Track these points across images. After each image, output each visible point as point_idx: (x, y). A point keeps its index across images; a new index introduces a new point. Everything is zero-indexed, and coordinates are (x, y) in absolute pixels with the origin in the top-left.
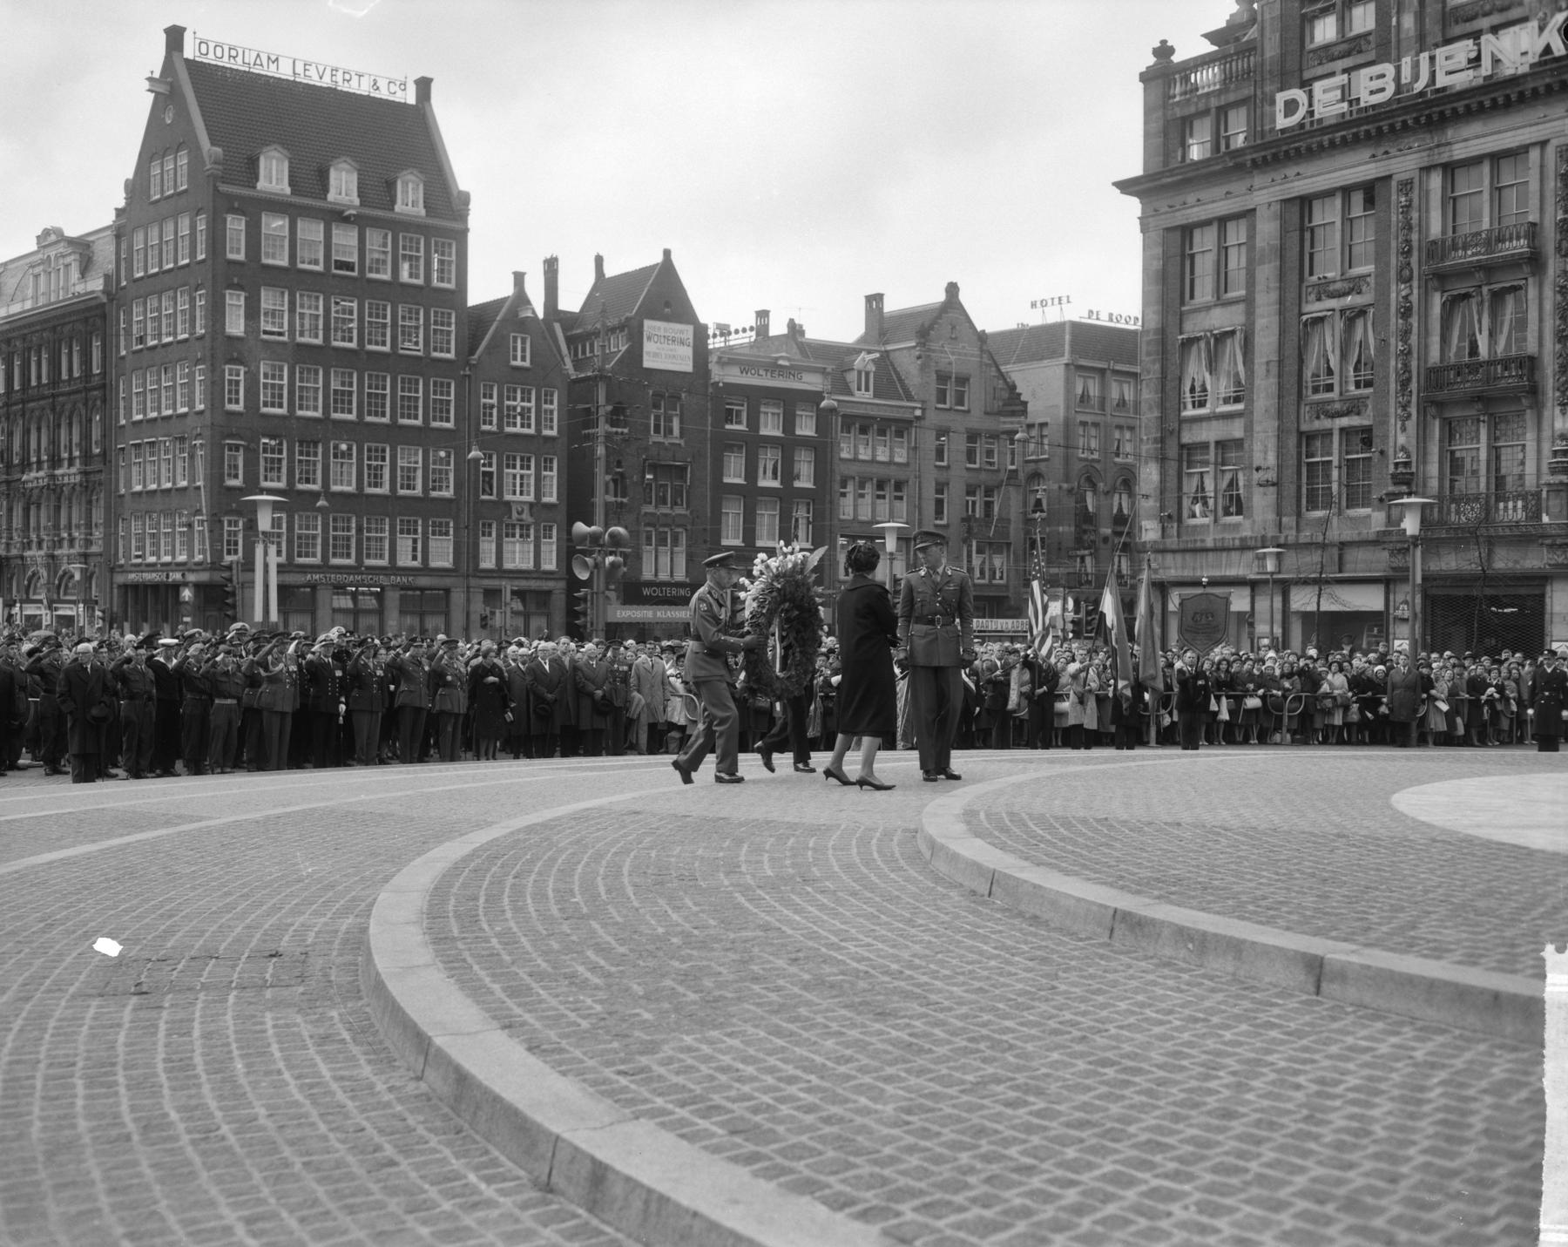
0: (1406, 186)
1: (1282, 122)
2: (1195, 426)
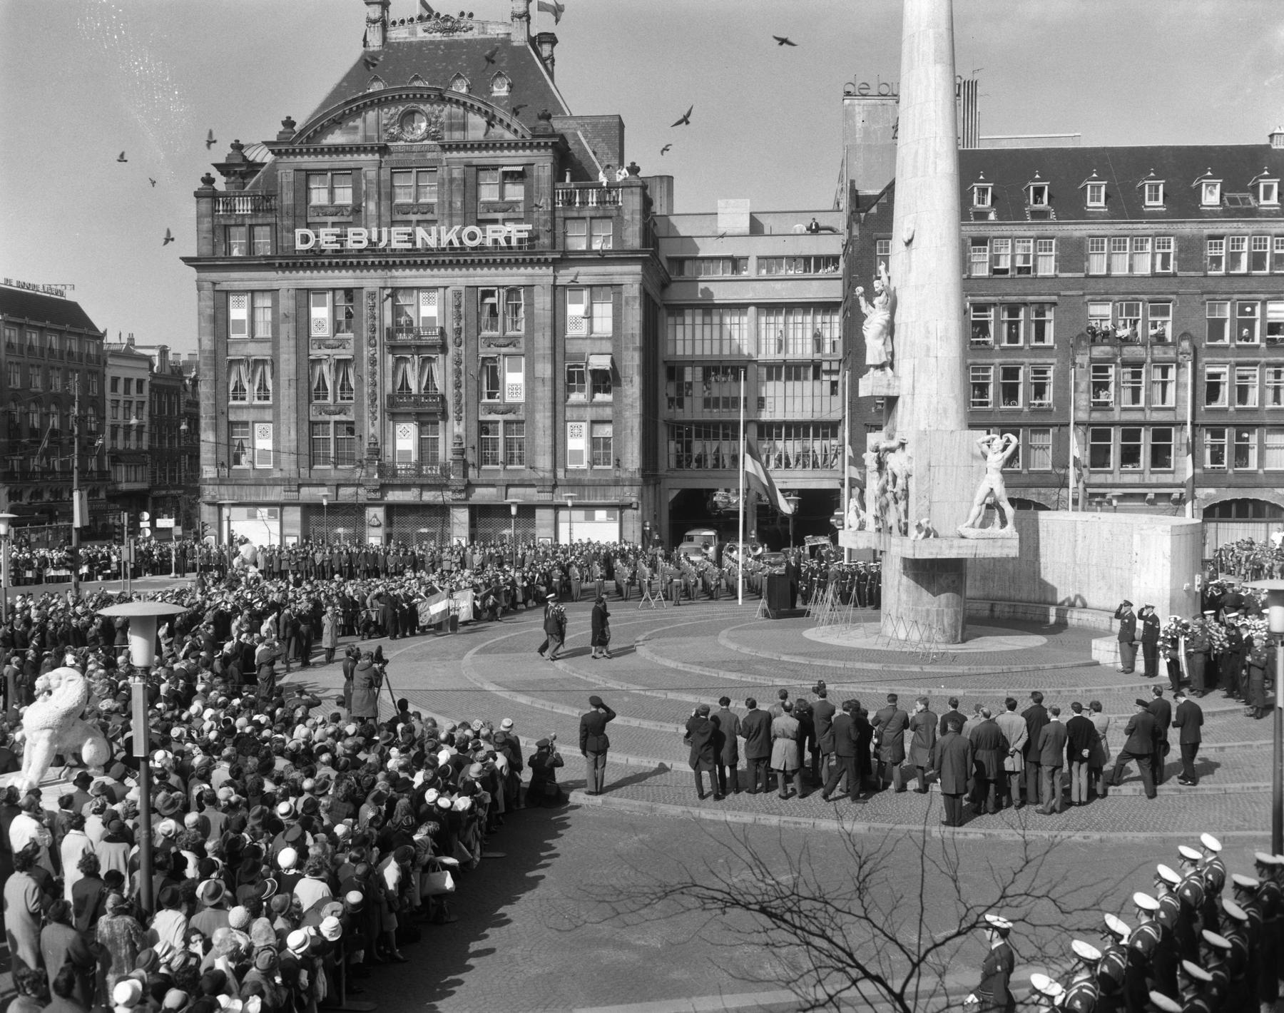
0: (372, 295)
1: (300, 246)
2: (239, 412)
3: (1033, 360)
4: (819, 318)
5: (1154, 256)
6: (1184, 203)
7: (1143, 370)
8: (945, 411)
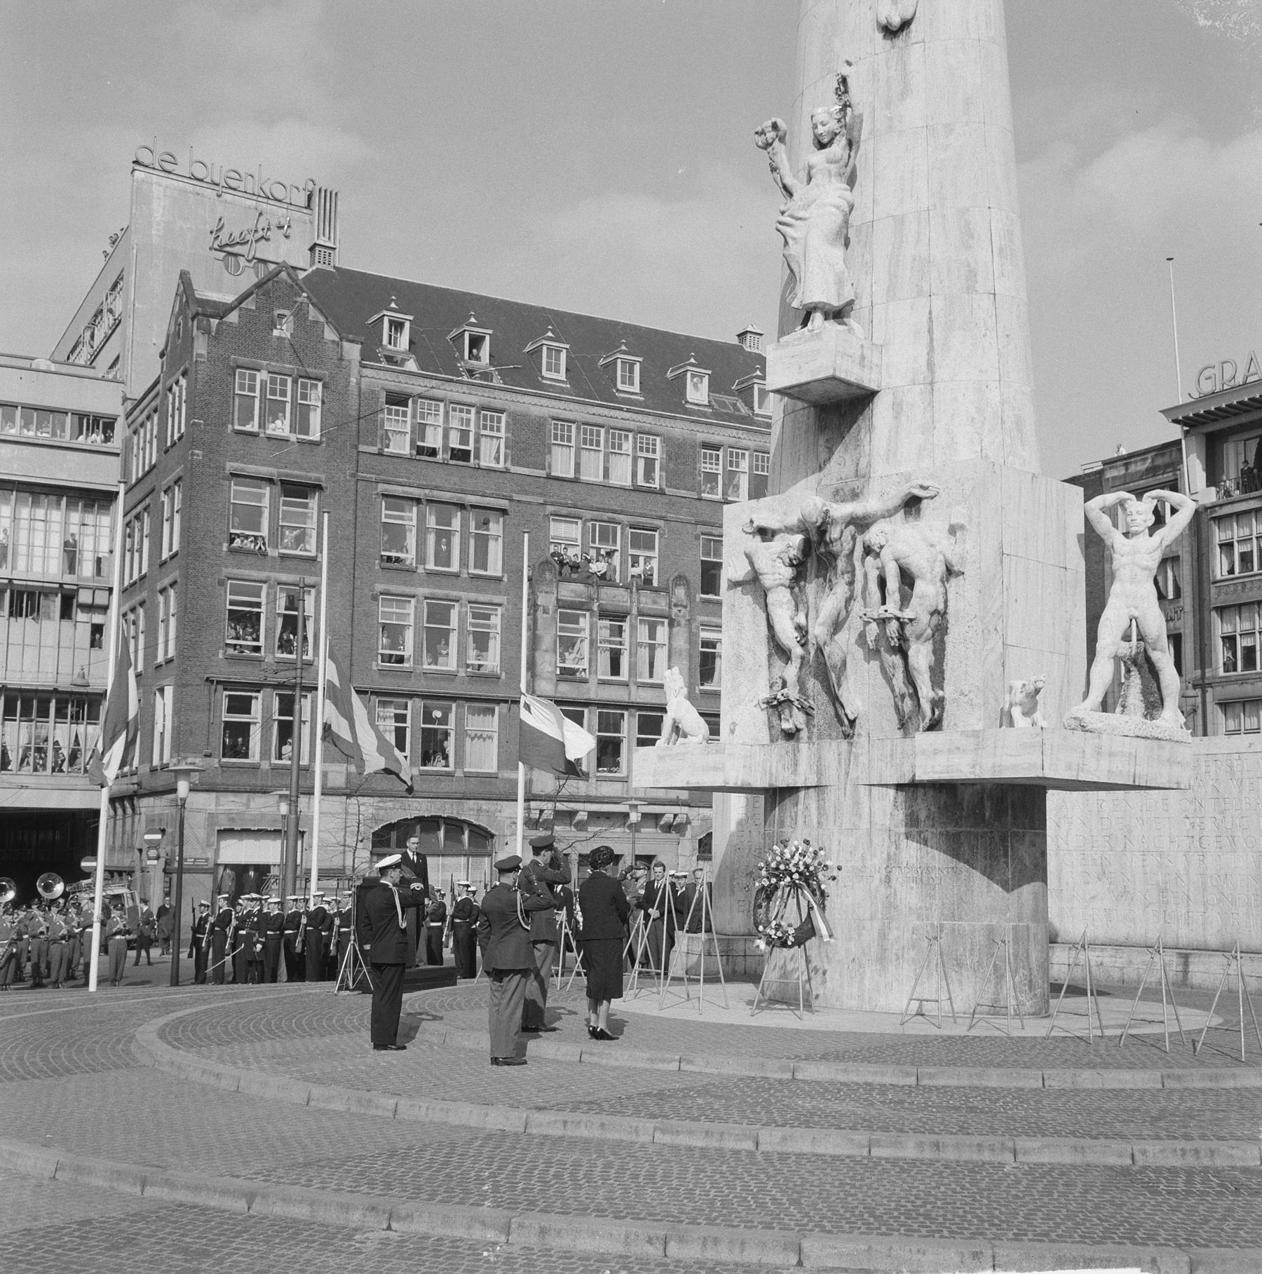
3: (473, 596)
4: (75, 517)
5: (635, 459)
6: (665, 395)
7: (626, 626)
8: (1019, 422)
